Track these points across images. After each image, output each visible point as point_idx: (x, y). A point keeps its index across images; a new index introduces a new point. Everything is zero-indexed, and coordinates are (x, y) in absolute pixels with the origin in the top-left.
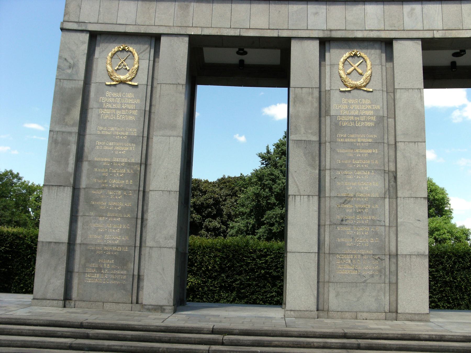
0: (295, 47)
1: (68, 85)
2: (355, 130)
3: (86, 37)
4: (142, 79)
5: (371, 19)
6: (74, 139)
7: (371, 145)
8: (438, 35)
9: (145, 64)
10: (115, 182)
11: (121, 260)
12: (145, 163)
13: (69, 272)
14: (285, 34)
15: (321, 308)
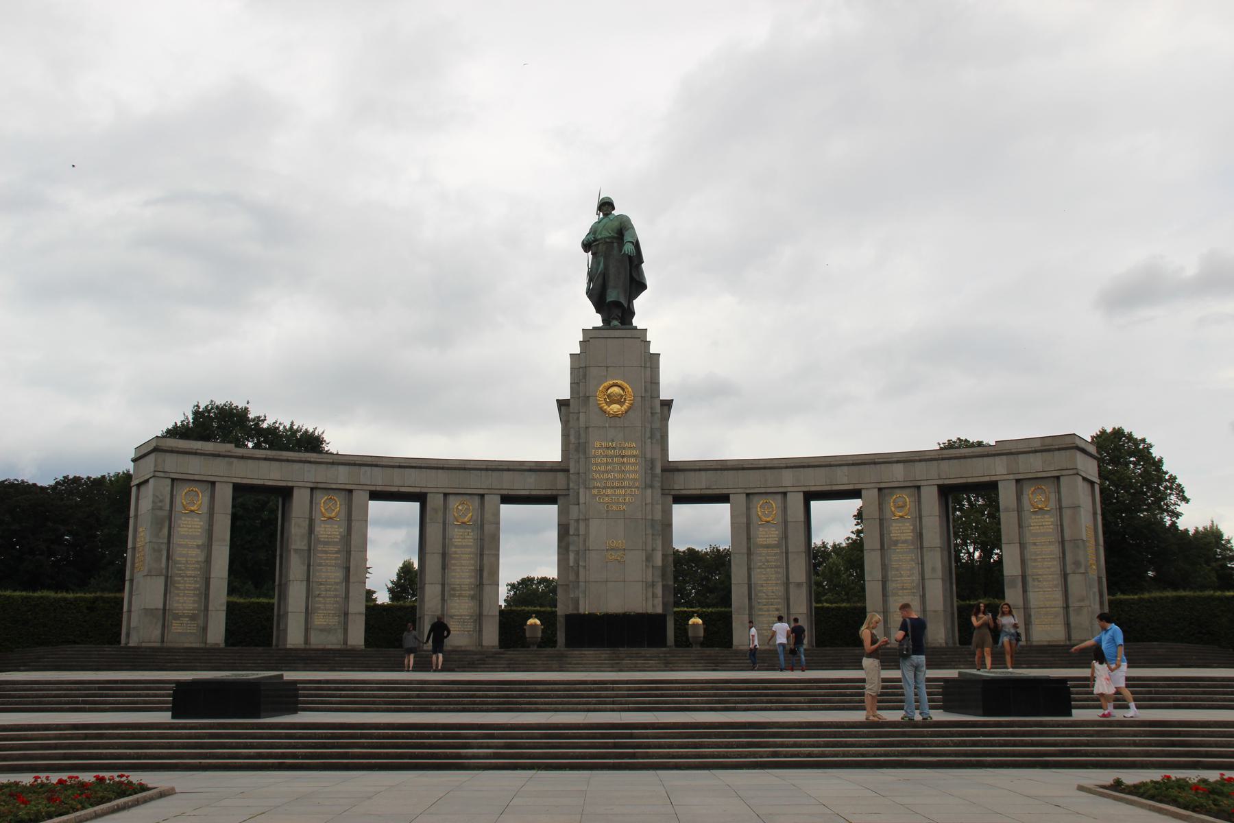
0: (296, 493)
1: (160, 513)
2: (327, 543)
3: (169, 481)
4: (205, 509)
5: (342, 476)
6: (164, 547)
7: (337, 552)
8: (379, 489)
9: (206, 500)
10: (189, 573)
11: (193, 618)
12: (208, 560)
13: (164, 626)
14: (290, 484)
15: (307, 640)
